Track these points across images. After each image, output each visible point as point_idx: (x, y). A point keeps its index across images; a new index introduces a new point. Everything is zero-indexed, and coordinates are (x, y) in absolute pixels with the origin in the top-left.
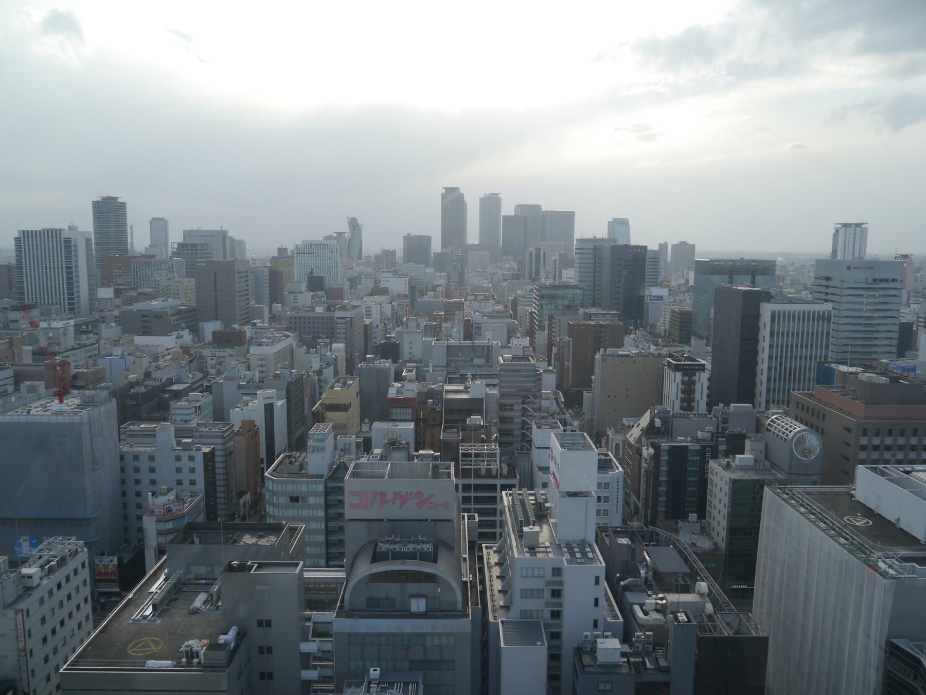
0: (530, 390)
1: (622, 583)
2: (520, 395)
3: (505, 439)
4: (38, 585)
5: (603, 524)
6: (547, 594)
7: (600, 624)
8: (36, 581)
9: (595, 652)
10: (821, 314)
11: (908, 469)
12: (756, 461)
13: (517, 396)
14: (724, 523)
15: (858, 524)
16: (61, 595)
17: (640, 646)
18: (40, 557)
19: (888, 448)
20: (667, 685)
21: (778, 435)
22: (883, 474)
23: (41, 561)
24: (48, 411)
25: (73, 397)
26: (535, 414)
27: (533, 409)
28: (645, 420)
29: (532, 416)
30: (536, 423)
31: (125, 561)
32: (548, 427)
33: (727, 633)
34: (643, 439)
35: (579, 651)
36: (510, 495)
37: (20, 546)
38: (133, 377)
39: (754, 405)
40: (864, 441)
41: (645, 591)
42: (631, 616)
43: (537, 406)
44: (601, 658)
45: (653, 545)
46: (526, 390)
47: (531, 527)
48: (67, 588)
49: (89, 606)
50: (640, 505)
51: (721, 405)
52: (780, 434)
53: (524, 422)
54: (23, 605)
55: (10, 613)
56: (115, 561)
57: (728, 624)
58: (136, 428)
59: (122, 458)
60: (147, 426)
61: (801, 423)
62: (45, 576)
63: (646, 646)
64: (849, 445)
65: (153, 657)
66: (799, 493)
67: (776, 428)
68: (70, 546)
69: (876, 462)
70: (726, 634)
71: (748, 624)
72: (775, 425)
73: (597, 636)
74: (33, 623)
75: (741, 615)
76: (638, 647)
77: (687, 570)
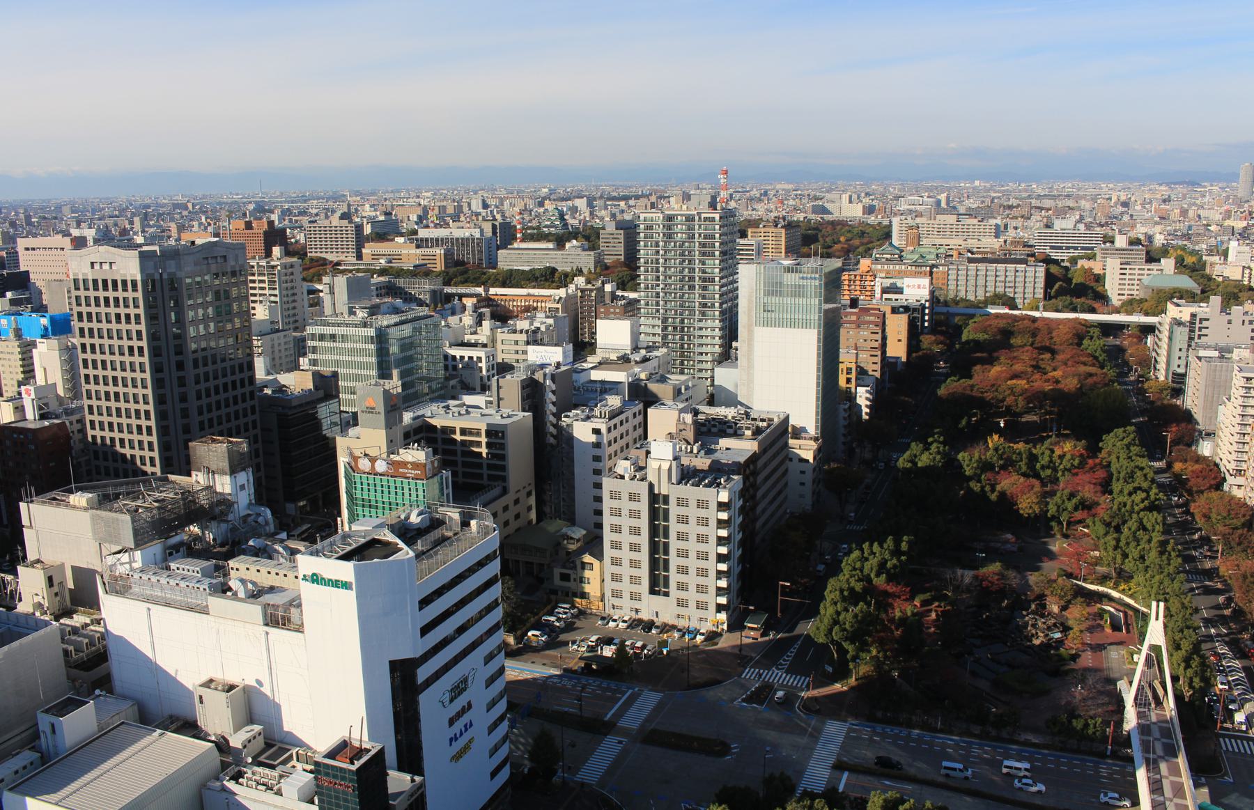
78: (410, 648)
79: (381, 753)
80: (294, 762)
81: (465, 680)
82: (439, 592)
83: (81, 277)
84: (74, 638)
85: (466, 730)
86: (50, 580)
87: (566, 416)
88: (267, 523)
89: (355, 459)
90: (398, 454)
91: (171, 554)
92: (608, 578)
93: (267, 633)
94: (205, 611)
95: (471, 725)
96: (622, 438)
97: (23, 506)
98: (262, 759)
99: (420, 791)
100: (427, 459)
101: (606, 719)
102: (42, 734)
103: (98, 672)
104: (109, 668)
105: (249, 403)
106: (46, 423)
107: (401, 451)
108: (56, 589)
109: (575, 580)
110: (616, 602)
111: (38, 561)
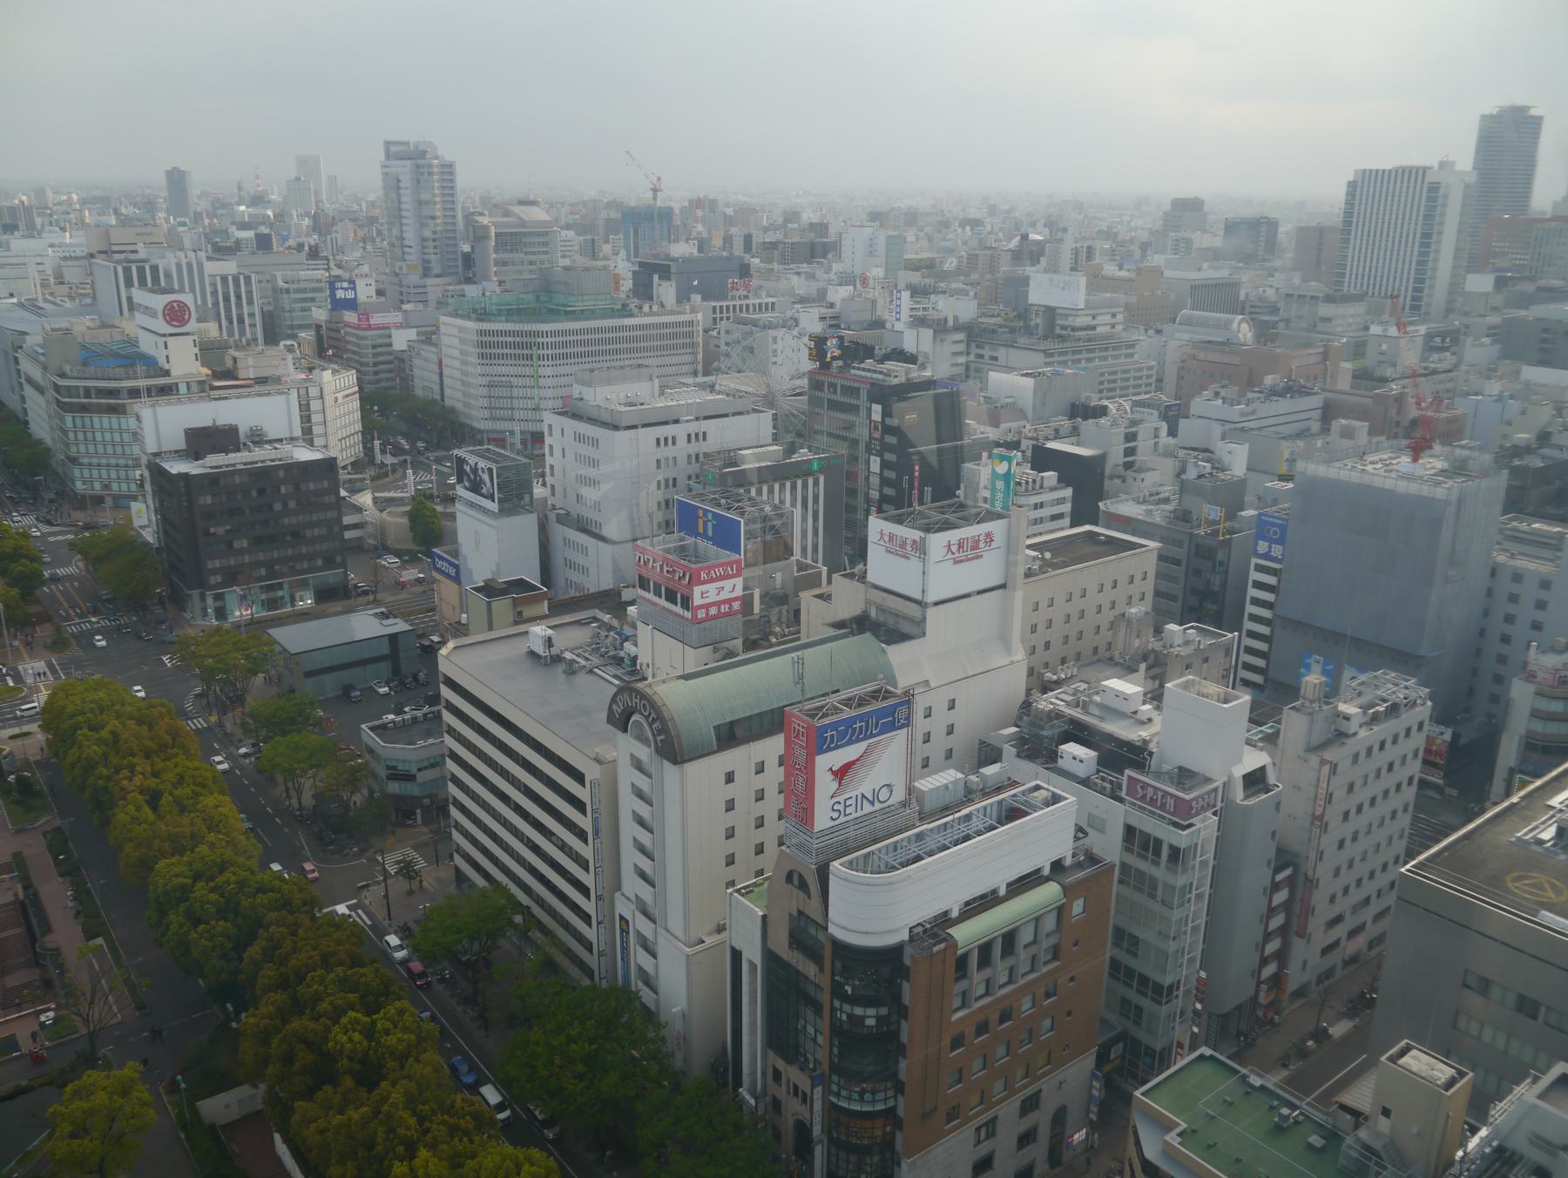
4: (1355, 734)
8: (1353, 727)
16: (1380, 759)
18: (1360, 694)
23: (1362, 700)
24: (1391, 471)
25: (1431, 456)
31: (1463, 741)
37: (1308, 667)
38: (1523, 437)
48: (1392, 753)
49: (1414, 788)
54: (1329, 755)
55: (1314, 760)
56: (1448, 736)
58: (1524, 526)
59: (1493, 573)
60: (1546, 527)
62: (1366, 723)
65: (1551, 908)
68: (1406, 691)
74: (1339, 787)
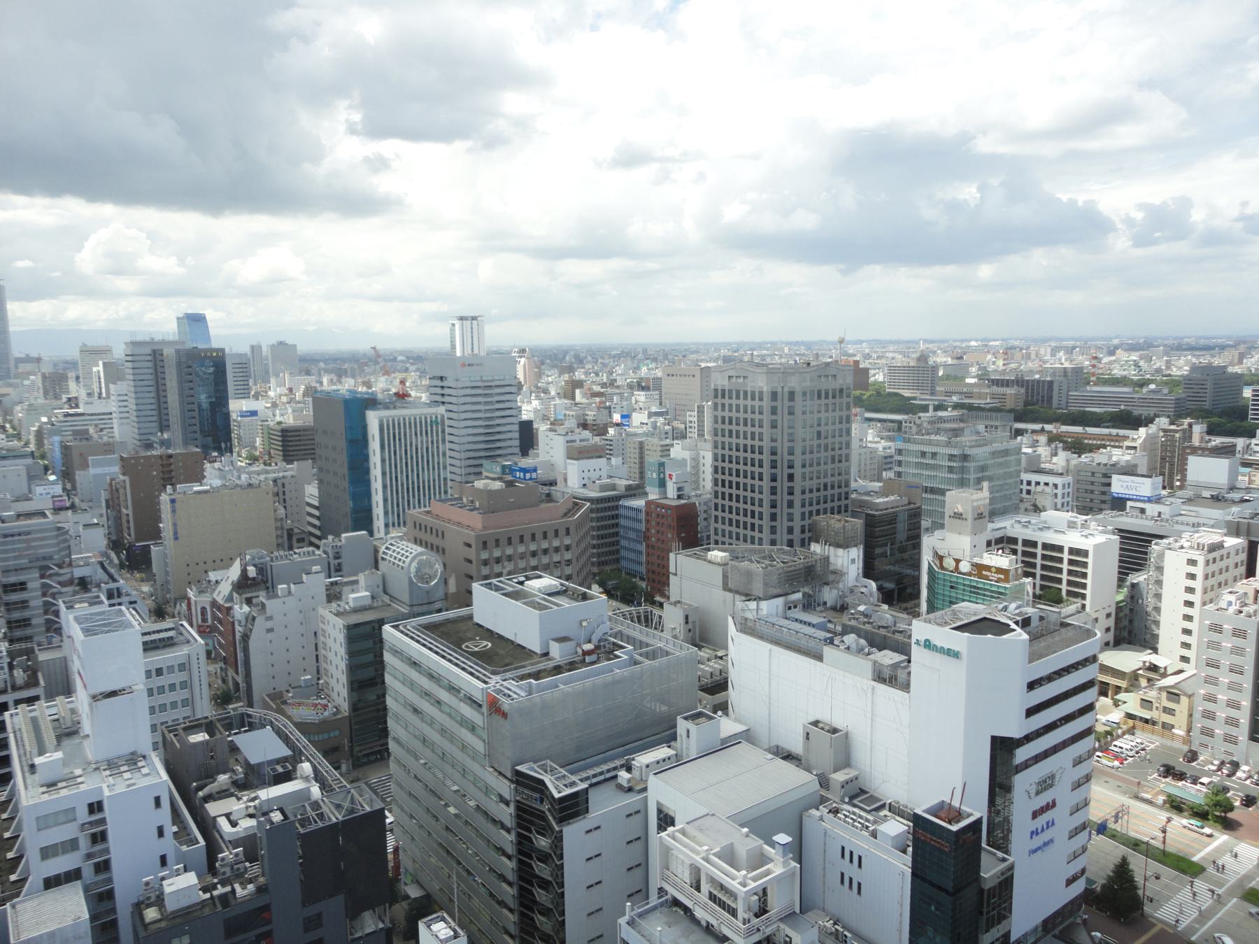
0: (51, 558)
1: (201, 794)
2: (35, 567)
3: (18, 633)
5: (173, 721)
6: (84, 844)
7: (170, 860)
9: (163, 900)
10: (434, 419)
11: (522, 579)
12: (373, 597)
13: (31, 568)
14: (343, 679)
15: (476, 649)
17: (227, 870)
19: (498, 561)
20: (266, 908)
21: (394, 564)
22: (497, 589)
26: (64, 590)
27: (60, 583)
28: (234, 572)
29: (60, 593)
30: (64, 602)
32: (86, 605)
33: (335, 817)
34: (235, 595)
35: (139, 907)
36: (17, 714)
39: (371, 533)
40: (485, 555)
41: (232, 795)
42: (216, 834)
43: (67, 577)
44: (171, 906)
45: (245, 731)
46: (44, 558)
47: (48, 755)
50: (240, 679)
51: (330, 537)
52: (397, 562)
53: (47, 604)
57: (338, 807)
61: (421, 545)
63: (236, 867)
64: (470, 562)
66: (414, 628)
67: (391, 556)
69: (486, 578)
70: (334, 820)
71: (360, 799)
72: (390, 552)
73: (163, 879)
75: (352, 791)
76: (224, 873)
77: (289, 753)
78: (1014, 727)
79: (979, 821)
80: (885, 812)
81: (1052, 777)
82: (1050, 678)
83: (720, 388)
84: (702, 667)
85: (1048, 827)
86: (687, 617)
87: (1156, 544)
88: (871, 594)
89: (941, 558)
90: (982, 557)
91: (790, 608)
92: (1197, 716)
93: (873, 688)
94: (819, 657)
95: (1053, 824)
96: (1221, 573)
97: (672, 556)
98: (856, 801)
99: (1010, 873)
100: (1010, 565)
101: (1195, 859)
102: (678, 738)
103: (719, 697)
104: (727, 696)
105: (843, 502)
106: (683, 502)
107: (985, 555)
108: (690, 626)
109: (1157, 708)
110: (1206, 739)
111: (679, 602)
